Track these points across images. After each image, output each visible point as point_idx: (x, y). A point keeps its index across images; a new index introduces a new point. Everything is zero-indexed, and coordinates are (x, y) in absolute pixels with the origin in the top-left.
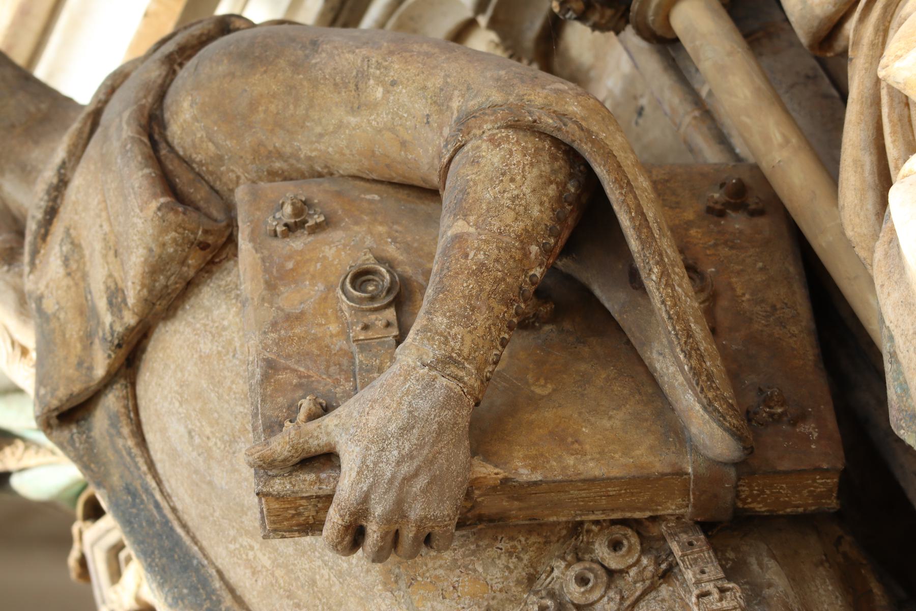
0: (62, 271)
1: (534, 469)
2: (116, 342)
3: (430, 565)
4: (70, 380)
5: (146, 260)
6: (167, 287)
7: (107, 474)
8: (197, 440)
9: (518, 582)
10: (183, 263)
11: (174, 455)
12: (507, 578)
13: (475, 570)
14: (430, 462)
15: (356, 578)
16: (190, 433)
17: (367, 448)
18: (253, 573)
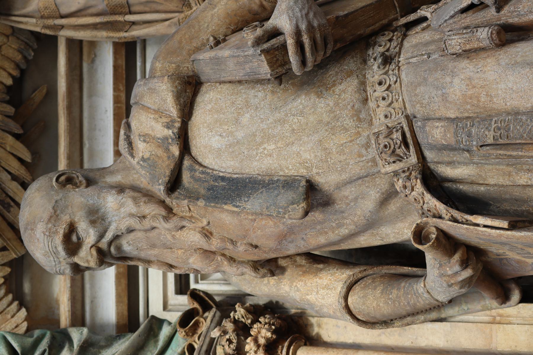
0: (145, 144)
1: (343, 11)
2: (177, 136)
3: (329, 79)
4: (168, 166)
5: (173, 96)
6: (185, 101)
7: (199, 193)
8: (224, 134)
9: (361, 64)
10: (186, 92)
11: (219, 152)
12: (356, 64)
13: (345, 69)
14: (310, 8)
15: (307, 106)
16: (220, 135)
17: (287, 13)
18: (270, 156)
